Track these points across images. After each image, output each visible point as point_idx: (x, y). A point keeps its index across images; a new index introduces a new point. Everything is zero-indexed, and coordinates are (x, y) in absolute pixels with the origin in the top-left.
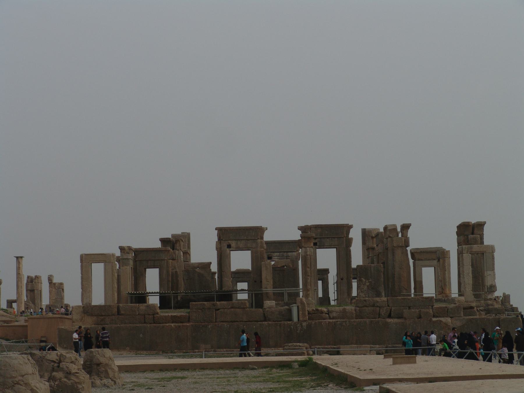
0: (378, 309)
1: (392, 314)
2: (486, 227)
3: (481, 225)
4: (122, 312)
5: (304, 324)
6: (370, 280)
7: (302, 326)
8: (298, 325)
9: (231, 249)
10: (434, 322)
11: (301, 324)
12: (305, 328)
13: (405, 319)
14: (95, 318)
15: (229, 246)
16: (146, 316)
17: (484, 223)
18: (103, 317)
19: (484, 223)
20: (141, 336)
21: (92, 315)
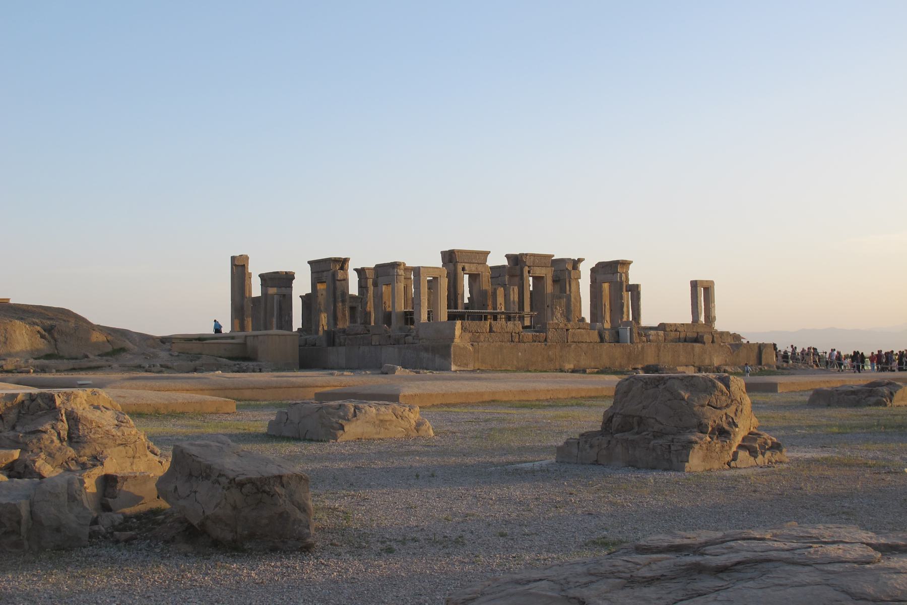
0: (679, 333)
1: (687, 339)
2: (631, 266)
3: (626, 264)
4: (494, 329)
5: (640, 346)
6: (563, 308)
7: (638, 348)
8: (635, 347)
9: (465, 272)
10: (722, 346)
11: (637, 346)
12: (640, 349)
13: (704, 343)
14: (470, 335)
15: (463, 269)
16: (513, 334)
17: (632, 262)
18: (478, 334)
19: (632, 262)
20: (520, 354)
21: (469, 332)
